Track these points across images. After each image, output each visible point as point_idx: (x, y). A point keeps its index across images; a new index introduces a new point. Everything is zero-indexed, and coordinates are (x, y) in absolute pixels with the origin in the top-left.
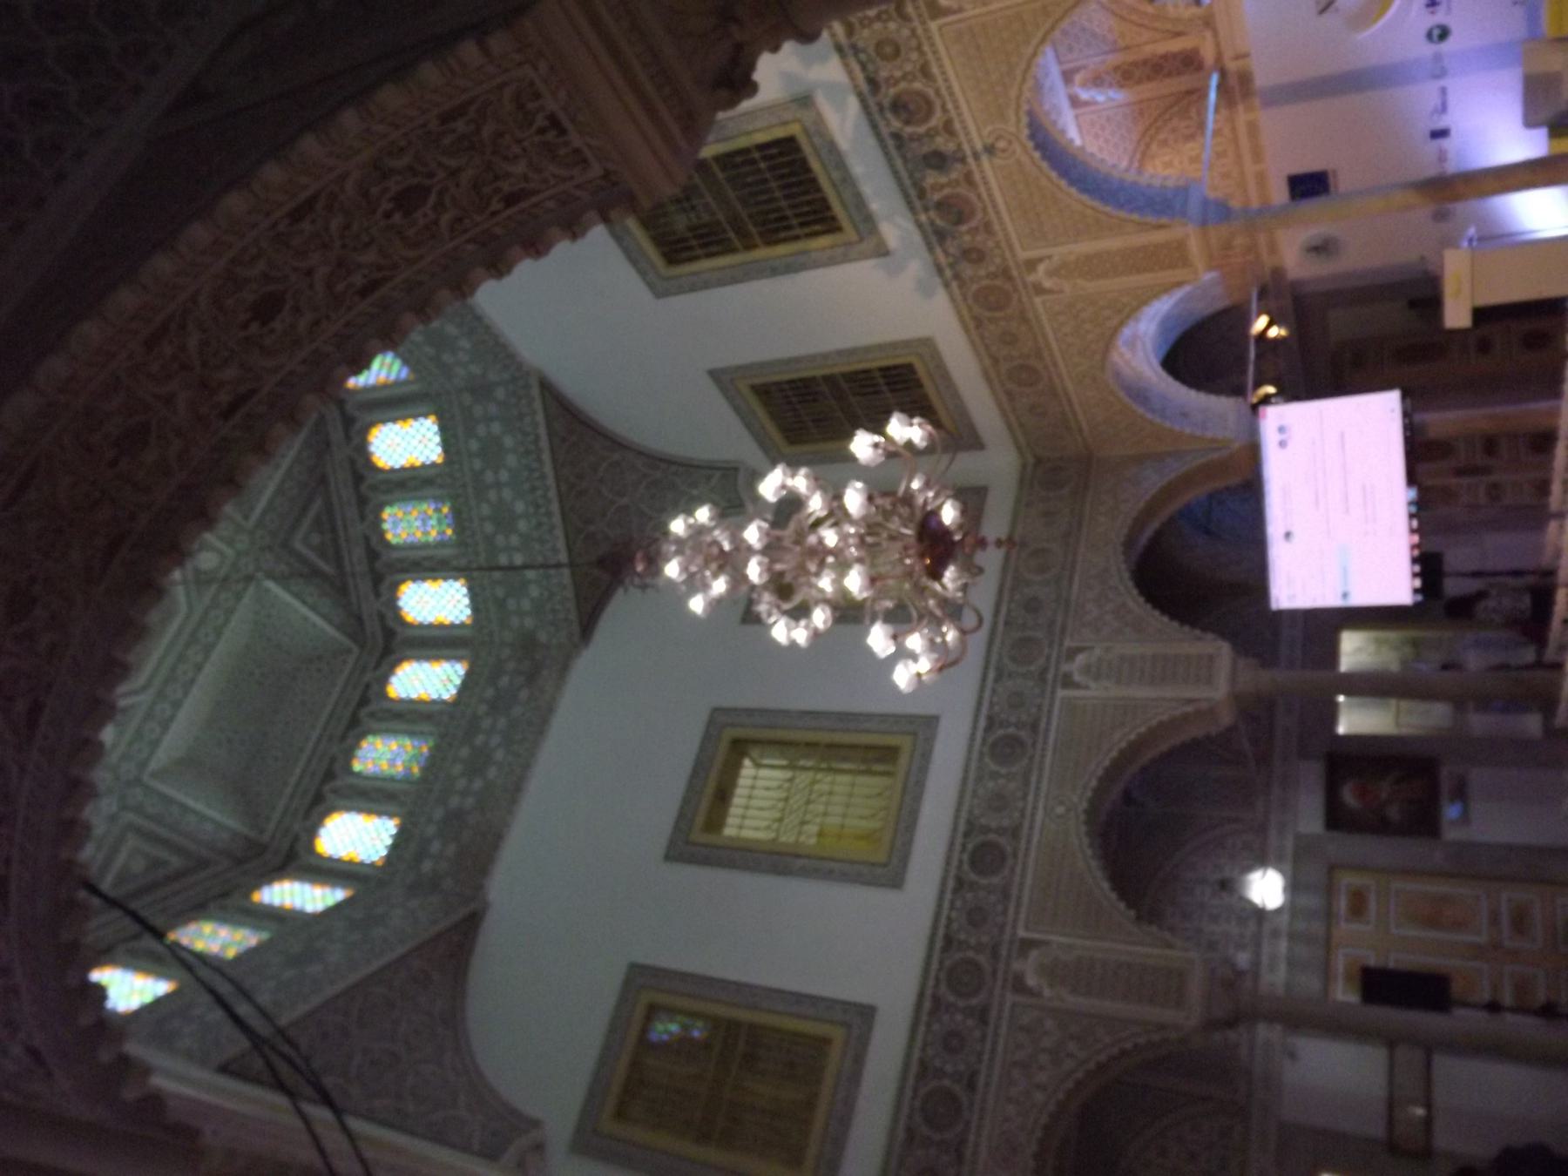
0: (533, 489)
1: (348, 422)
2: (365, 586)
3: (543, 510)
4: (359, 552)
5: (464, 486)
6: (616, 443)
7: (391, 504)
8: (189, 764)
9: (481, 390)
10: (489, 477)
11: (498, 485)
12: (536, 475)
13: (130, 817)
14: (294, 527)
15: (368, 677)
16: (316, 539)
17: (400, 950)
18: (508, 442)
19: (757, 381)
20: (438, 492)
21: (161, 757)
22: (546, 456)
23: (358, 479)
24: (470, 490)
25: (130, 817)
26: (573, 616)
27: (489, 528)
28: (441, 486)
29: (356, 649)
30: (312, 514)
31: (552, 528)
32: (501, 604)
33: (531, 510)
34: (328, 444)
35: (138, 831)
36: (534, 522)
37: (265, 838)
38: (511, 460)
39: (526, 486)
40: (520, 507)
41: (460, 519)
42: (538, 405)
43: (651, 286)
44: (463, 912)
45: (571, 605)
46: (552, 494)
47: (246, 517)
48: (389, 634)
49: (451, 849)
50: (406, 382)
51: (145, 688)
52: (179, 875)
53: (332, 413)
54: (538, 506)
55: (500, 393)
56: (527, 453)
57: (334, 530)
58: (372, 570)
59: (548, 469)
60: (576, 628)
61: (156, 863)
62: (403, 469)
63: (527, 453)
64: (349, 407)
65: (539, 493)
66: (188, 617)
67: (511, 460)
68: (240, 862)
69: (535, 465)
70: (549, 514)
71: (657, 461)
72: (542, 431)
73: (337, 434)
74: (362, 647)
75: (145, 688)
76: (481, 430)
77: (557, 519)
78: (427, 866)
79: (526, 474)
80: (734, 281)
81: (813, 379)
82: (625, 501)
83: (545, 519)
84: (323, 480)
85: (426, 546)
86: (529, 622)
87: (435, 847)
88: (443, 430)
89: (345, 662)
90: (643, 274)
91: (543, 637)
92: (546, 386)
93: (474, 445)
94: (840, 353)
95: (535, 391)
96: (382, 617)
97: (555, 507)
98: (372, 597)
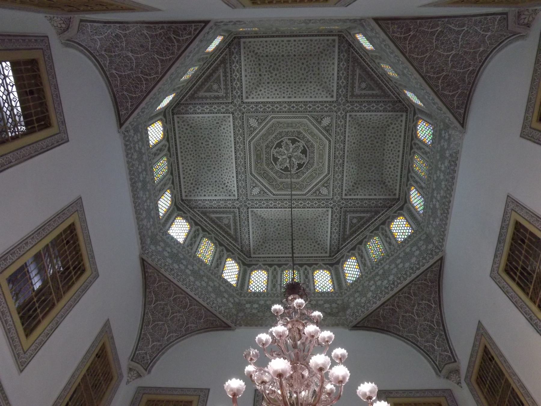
0: (400, 279)
1: (401, 208)
2: (350, 246)
3: (392, 286)
4: (360, 237)
5: (392, 255)
6: (439, 303)
7: (379, 237)
8: (263, 222)
9: (428, 239)
10: (399, 261)
11: (397, 266)
12: (405, 276)
13: (236, 210)
14: (353, 212)
15: (321, 263)
16: (355, 221)
17: (205, 304)
18: (414, 260)
19: (488, 346)
20: (387, 249)
21: (259, 211)
22: (414, 276)
23: (383, 223)
24: (391, 258)
25: (236, 210)
26: (359, 319)
27: (381, 272)
28: (390, 248)
29: (328, 255)
30: (362, 215)
31: (388, 293)
32: (356, 291)
33: (391, 282)
34: (390, 207)
35: (235, 217)
36: (387, 286)
37: (252, 256)
38: (407, 265)
39: (400, 276)
40: (391, 278)
41: (380, 262)
42: (432, 262)
43: (492, 270)
44: (229, 322)
45: (363, 316)
46: (400, 286)
47: (346, 195)
48: (338, 263)
49: (255, 311)
50: (420, 215)
51: (274, 195)
52: (229, 235)
53: (401, 203)
54: (393, 284)
55: (430, 246)
56: (412, 269)
57: (362, 225)
58: (356, 245)
59: (409, 279)
60: (355, 323)
61: (229, 226)
62: (392, 233)
63: (412, 269)
64: (406, 205)
65: (399, 281)
66: (302, 195)
67: (407, 265)
68: (242, 251)
69: (408, 273)
70: (392, 289)
71: (442, 323)
72: (422, 269)
73: (395, 208)
74: (330, 256)
75: (274, 195)
76: (414, 249)
77: (392, 293)
78: (248, 306)
79: (404, 273)
80: (515, 304)
81: (503, 375)
82: (416, 318)
83: (390, 288)
84: (377, 213)
85: (368, 255)
86: (352, 305)
87: (256, 306)
88: (409, 237)
89: (321, 253)
90: (494, 262)
91: (349, 312)
92: (442, 259)
93: (408, 250)
94: (519, 381)
95: (436, 258)
96: (343, 257)
97: (396, 290)
98: (348, 250)
